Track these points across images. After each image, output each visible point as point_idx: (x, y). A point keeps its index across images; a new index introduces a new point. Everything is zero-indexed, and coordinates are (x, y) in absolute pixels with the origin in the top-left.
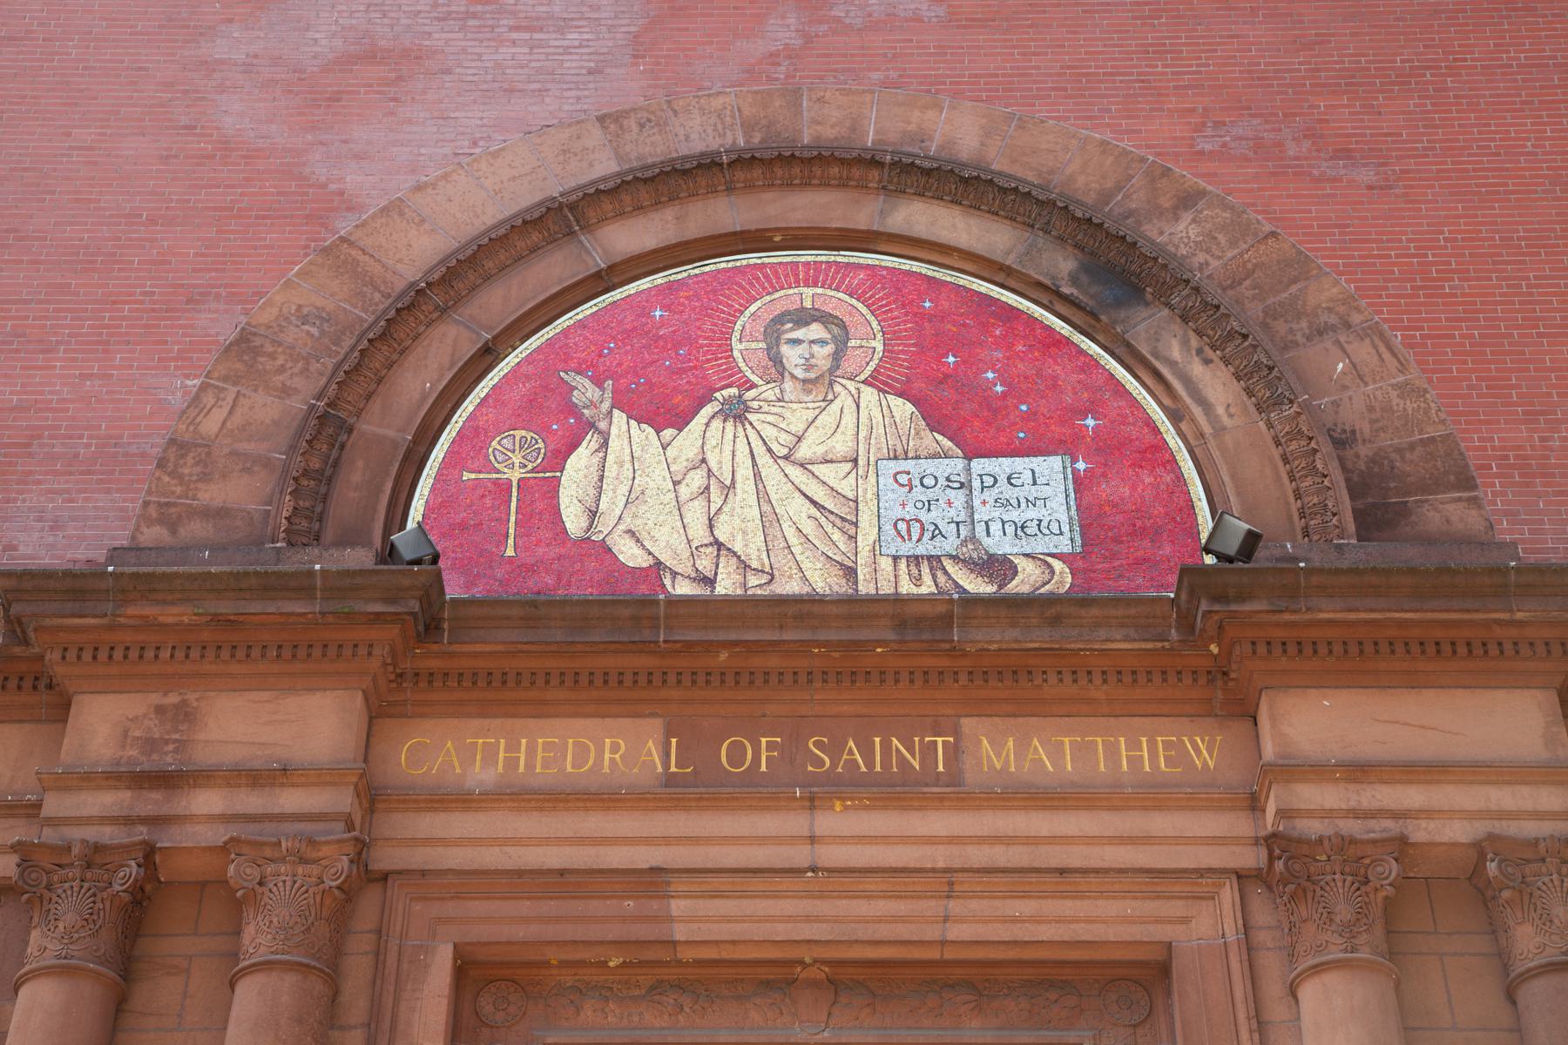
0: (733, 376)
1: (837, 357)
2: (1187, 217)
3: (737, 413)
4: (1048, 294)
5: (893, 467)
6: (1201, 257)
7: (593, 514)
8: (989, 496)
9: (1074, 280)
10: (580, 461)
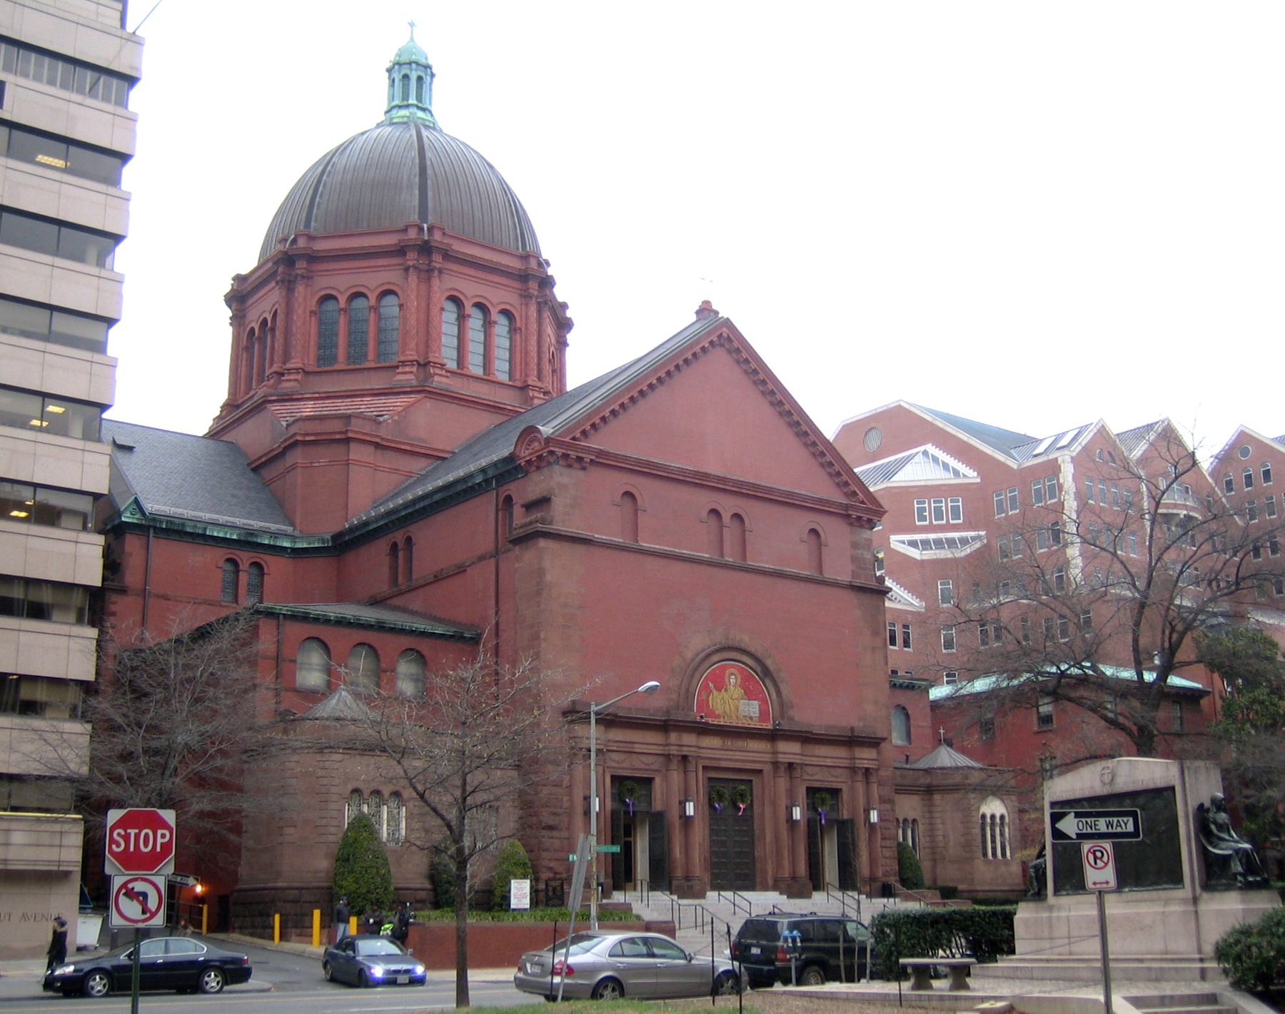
10: (711, 697)
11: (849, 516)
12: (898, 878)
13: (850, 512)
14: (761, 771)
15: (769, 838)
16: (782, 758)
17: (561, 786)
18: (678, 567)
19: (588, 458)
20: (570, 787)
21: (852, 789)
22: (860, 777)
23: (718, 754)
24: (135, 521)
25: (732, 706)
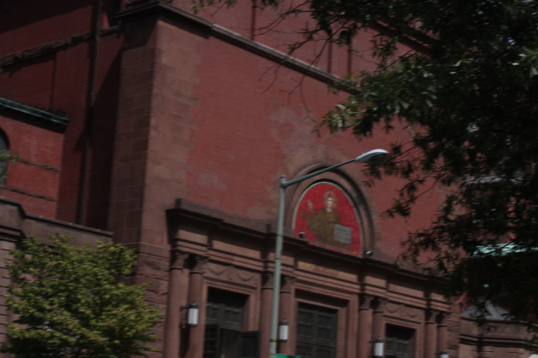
16: (369, 290)
20: (169, 294)
22: (432, 320)
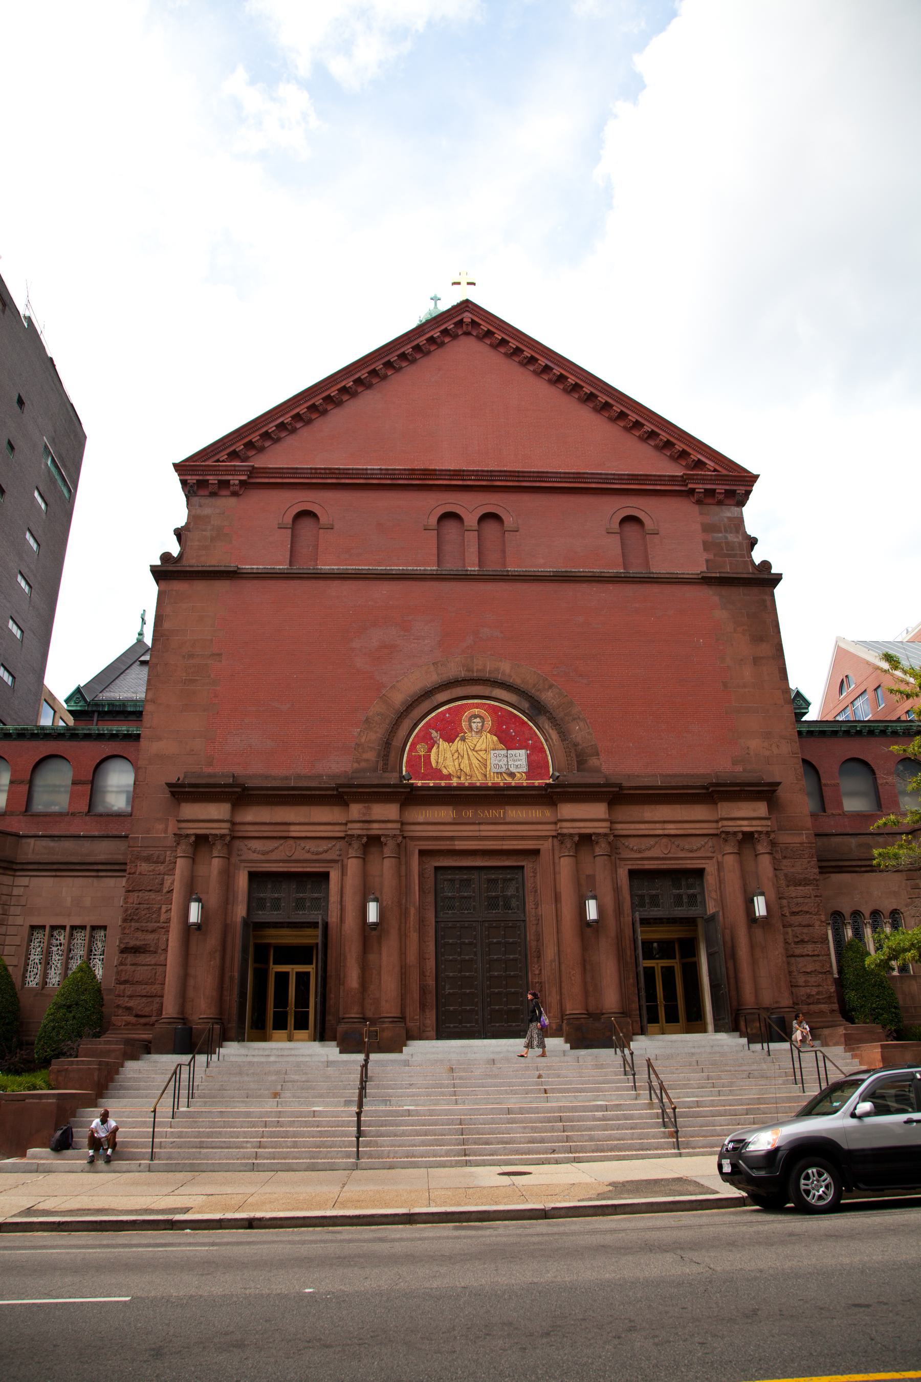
0: (462, 731)
1: (482, 726)
2: (550, 691)
3: (463, 739)
4: (523, 712)
5: (493, 752)
6: (553, 701)
7: (437, 762)
8: (511, 759)
9: (528, 709)
10: (434, 750)
11: (692, 492)
12: (836, 1006)
13: (690, 486)
14: (536, 852)
15: (550, 952)
16: (567, 828)
17: (159, 891)
18: (383, 590)
19: (235, 479)
21: (720, 869)
23: (448, 831)
24: (79, 708)
25: (475, 762)
